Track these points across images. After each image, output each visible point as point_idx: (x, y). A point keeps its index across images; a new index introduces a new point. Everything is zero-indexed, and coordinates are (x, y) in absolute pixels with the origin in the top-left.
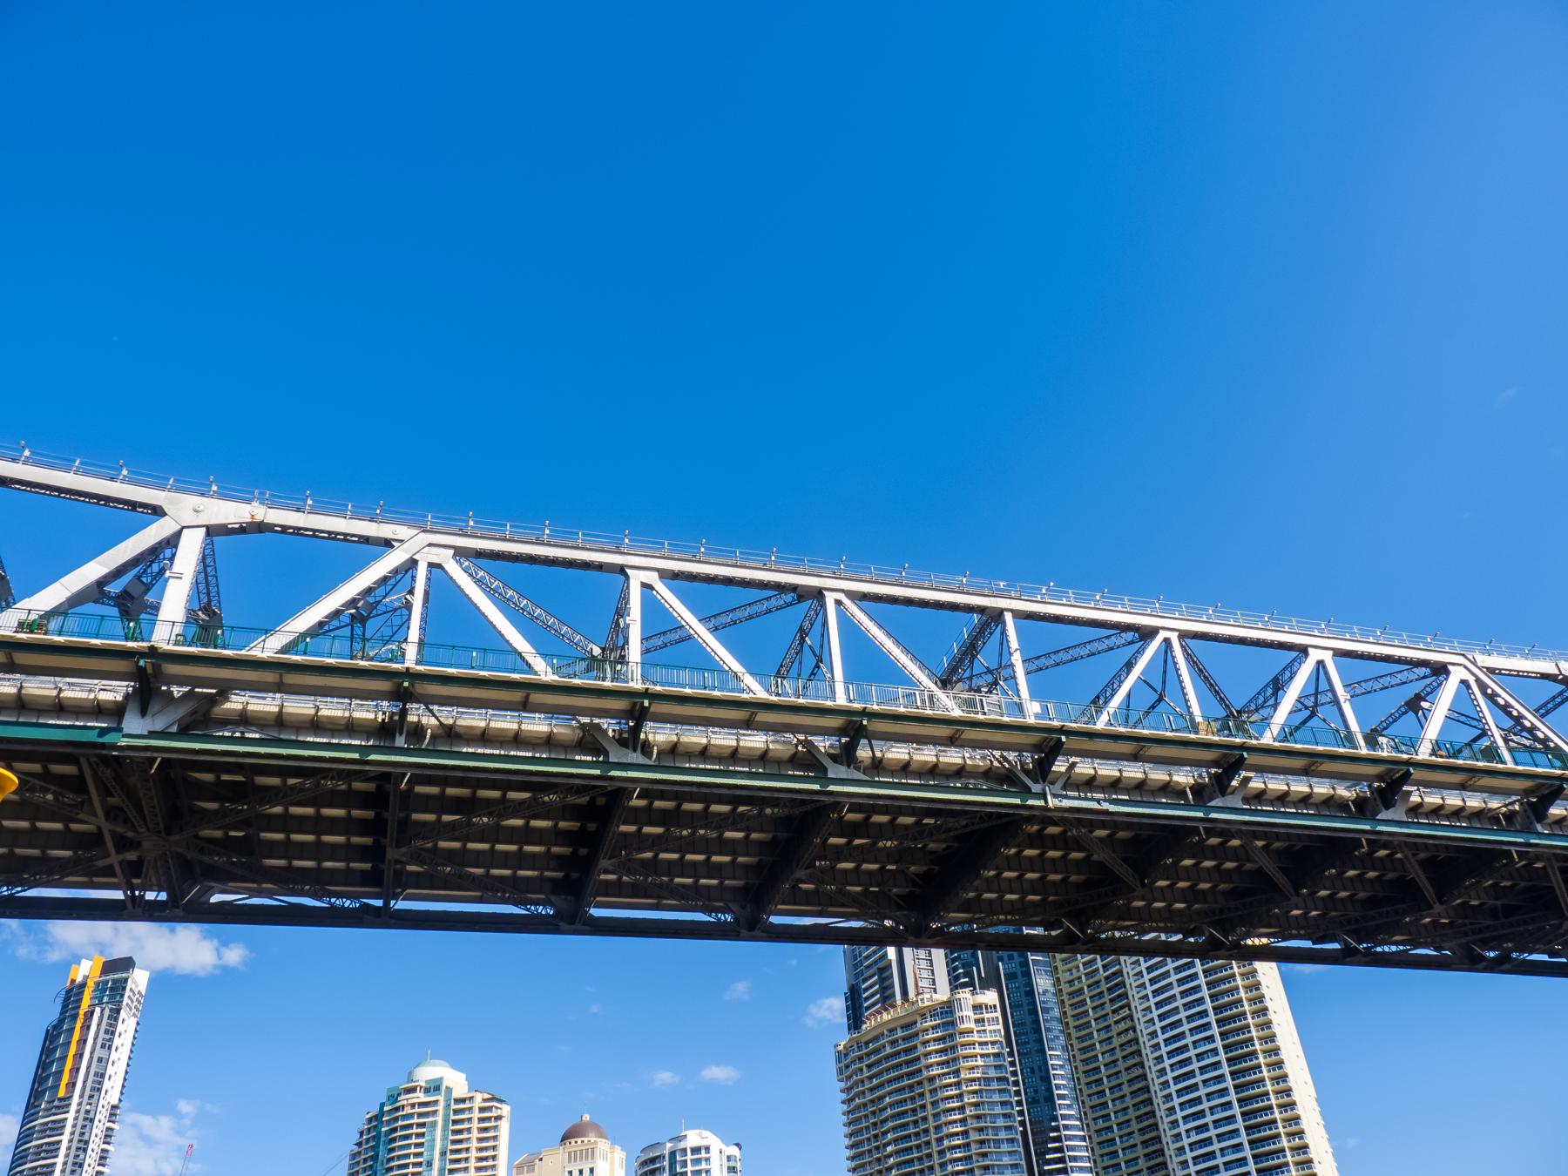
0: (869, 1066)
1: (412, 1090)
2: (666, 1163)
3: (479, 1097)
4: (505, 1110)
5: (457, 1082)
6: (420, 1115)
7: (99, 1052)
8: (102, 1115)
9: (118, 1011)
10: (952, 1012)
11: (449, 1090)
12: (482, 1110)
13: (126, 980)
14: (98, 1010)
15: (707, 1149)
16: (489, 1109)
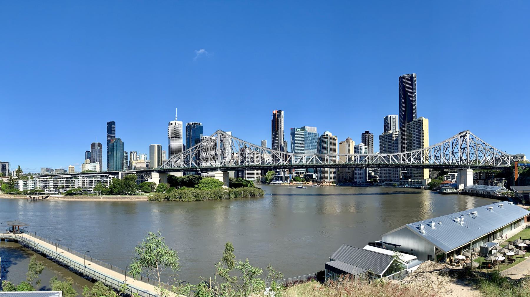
0: (382, 139)
1: (324, 135)
2: (357, 148)
3: (333, 137)
4: (337, 138)
5: (330, 134)
6: (326, 139)
7: (280, 124)
8: (282, 132)
9: (281, 118)
10: (392, 135)
11: (329, 136)
12: (334, 138)
13: (281, 114)
14: (278, 118)
15: (362, 147)
16: (335, 138)
